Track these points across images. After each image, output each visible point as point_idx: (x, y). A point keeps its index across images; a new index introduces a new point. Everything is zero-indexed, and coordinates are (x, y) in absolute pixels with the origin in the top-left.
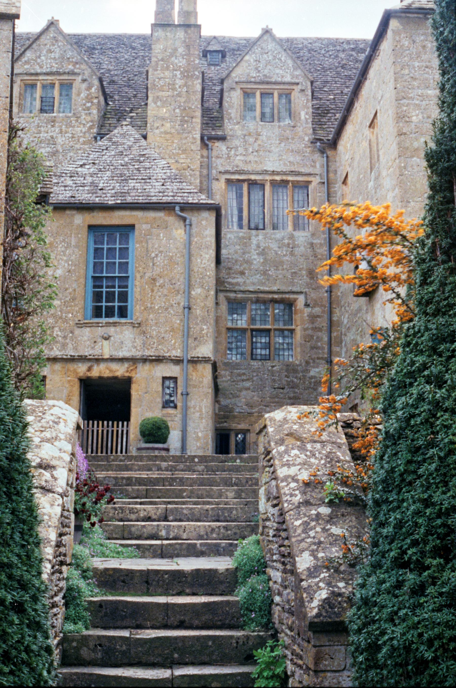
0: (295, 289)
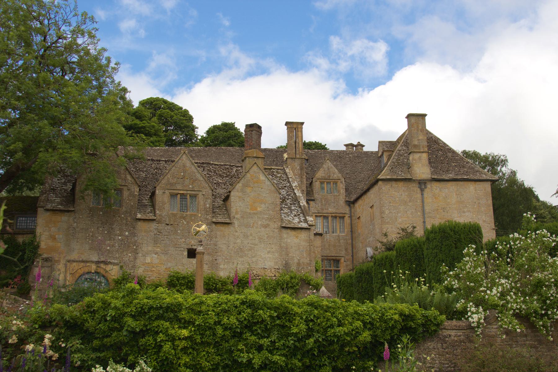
0: (340, 255)
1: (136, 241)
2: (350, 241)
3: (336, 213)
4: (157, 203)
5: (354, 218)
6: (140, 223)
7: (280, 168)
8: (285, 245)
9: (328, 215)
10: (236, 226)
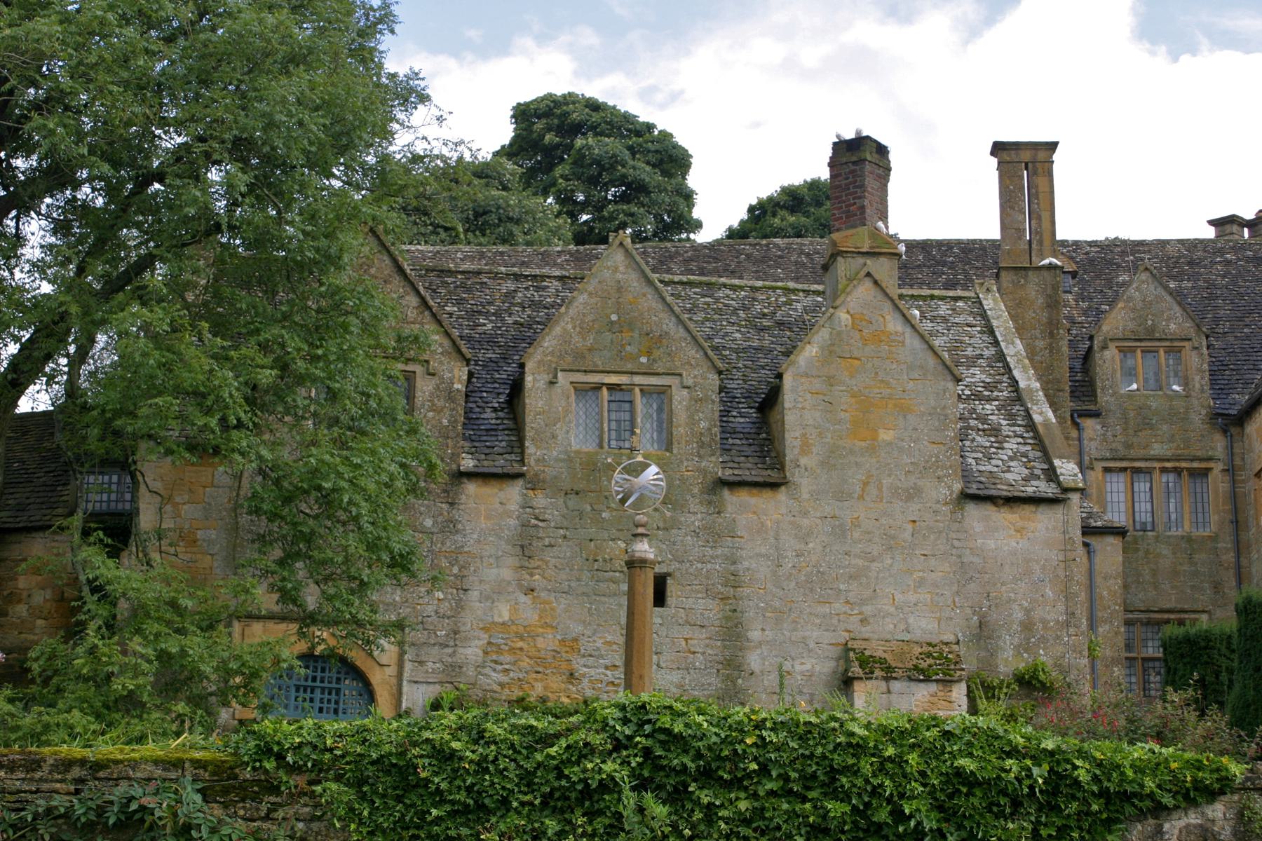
0: (1195, 607)
1: (459, 550)
2: (1230, 557)
3: (1178, 459)
4: (529, 419)
5: (1242, 476)
6: (471, 488)
7: (959, 293)
8: (976, 560)
9: (1148, 464)
10: (805, 496)
